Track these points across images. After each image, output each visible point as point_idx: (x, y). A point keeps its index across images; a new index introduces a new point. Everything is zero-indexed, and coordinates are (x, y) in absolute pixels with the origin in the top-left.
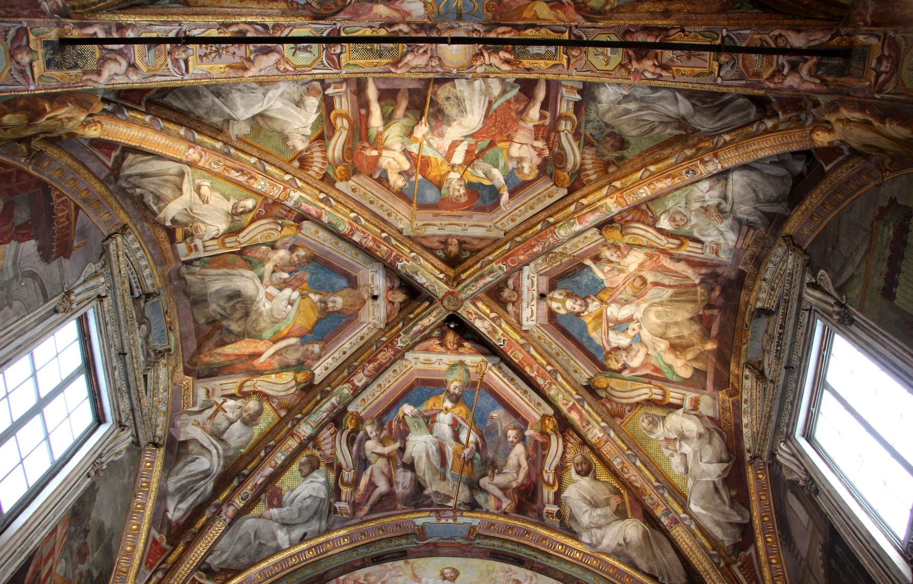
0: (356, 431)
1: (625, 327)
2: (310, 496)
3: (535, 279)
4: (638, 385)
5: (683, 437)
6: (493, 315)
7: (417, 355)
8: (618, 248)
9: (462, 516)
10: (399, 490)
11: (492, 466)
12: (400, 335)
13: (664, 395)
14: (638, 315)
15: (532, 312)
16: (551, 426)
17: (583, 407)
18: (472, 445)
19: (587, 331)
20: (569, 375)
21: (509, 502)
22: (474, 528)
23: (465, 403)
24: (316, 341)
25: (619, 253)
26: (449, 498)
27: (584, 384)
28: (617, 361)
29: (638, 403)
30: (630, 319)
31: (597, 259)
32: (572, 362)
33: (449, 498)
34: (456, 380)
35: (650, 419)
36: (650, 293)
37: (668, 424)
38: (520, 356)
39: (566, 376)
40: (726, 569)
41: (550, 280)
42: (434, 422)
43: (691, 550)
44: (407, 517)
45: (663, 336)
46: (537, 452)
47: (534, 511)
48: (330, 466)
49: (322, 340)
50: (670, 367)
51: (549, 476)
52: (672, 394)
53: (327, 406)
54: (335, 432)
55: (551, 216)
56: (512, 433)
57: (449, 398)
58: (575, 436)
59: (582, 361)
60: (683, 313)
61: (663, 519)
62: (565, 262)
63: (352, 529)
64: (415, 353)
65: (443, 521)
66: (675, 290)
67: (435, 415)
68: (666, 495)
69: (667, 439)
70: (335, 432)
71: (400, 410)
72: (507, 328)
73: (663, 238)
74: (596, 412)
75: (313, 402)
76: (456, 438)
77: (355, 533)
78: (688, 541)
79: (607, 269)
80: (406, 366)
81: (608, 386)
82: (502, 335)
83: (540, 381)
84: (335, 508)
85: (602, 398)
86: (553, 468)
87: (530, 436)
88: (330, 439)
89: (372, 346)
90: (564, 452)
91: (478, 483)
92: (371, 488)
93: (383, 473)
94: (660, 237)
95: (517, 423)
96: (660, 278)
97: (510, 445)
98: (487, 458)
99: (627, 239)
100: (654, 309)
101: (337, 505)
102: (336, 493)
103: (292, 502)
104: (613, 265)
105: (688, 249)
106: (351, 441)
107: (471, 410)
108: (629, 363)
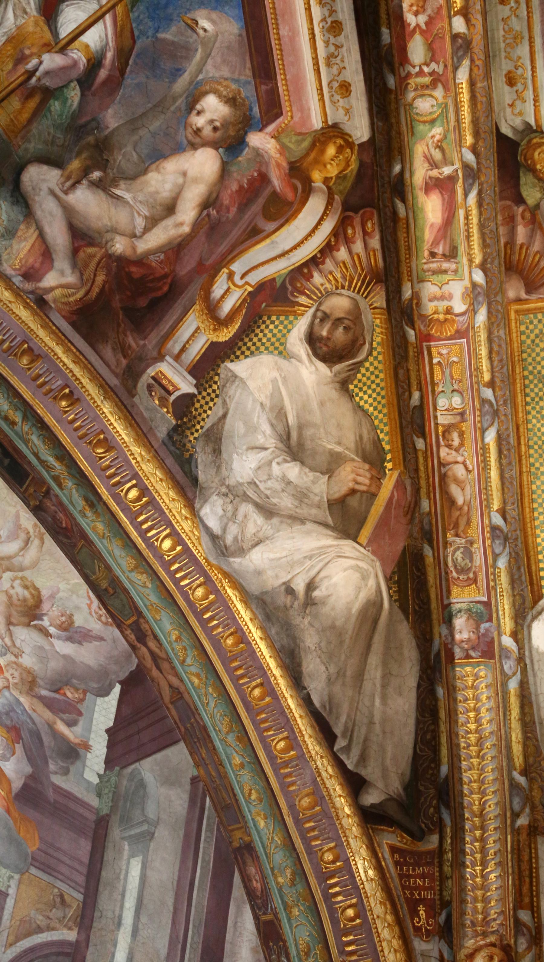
11: (93, 154)
16: (333, 171)
18: (77, 55)
20: (487, 76)
21: (71, 278)
27: (506, 130)
32: (523, 50)
40: (523, 837)
43: (480, 742)
46: (248, 206)
47: (123, 349)
51: (228, 292)
58: (375, 242)
61: (459, 622)
68: (502, 563)
78: (486, 716)
85: (520, 200)
86: (255, 278)
87: (258, 153)
90: (314, 262)
91: (20, 170)
95: (248, 93)
98: (96, 124)
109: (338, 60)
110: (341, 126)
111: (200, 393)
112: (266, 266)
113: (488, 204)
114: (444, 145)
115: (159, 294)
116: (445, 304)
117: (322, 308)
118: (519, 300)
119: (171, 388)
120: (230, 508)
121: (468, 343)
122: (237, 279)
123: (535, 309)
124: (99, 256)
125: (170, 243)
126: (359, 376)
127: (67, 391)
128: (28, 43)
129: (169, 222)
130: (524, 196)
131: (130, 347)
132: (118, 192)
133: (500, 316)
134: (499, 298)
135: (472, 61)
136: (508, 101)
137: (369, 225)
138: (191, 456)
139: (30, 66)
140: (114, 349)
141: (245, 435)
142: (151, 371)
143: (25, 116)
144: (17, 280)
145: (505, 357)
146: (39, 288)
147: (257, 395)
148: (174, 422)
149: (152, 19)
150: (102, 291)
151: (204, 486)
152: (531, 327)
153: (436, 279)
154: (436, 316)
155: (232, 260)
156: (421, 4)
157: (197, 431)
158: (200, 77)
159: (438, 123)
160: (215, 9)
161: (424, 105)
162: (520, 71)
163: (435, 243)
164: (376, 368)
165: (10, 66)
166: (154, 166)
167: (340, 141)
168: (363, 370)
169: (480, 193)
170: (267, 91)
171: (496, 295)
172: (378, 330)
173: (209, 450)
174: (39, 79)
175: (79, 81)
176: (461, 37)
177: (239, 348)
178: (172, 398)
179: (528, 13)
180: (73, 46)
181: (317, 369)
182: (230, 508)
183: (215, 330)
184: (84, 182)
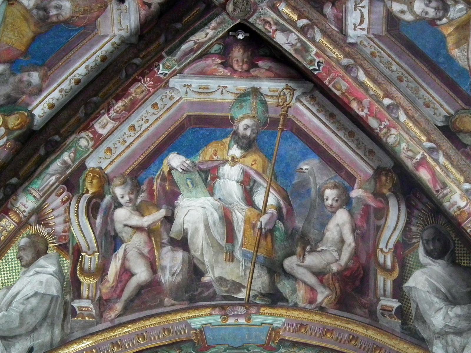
0: (100, 195)
2: (36, 294)
6: (302, 22)
7: (188, 81)
9: (258, 313)
10: (166, 278)
11: (302, 241)
12: (161, 58)
15: (362, 16)
16: (389, 185)
17: (437, 161)
18: (271, 211)
19: (445, 47)
21: (327, 292)
22: (275, 330)
23: (261, 150)
24: (34, 67)
26: (239, 287)
27: (440, 124)
32: (422, 92)
33: (239, 287)
34: (248, 116)
38: (344, 85)
39: (412, 111)
42: (216, 177)
44: (178, 316)
47: (363, 306)
48: (63, 248)
49: (43, 65)
53: (57, 165)
54: (69, 199)
56: (330, 194)
57: (237, 143)
58: (425, 200)
59: (436, 91)
63: (99, 338)
64: (185, 77)
65: (231, 321)
67: (217, 168)
70: (69, 199)
71: (165, 162)
72: (325, 42)
74: (456, 167)
75: (34, 159)
76: (249, 199)
77: (103, 344)
80: (171, 98)
82: (317, 54)
83: (373, 123)
84: (73, 308)
87: (358, 198)
88: (62, 209)
89: (119, 72)
91: (282, 265)
92: (125, 277)
93: (141, 254)
95: (339, 180)
97: (328, 211)
98: (295, 229)
101: (76, 304)
102: (73, 286)
103: (10, 304)
106: (92, 210)
107: (270, 160)
109: (361, 144)
110: (380, 166)
111: (402, 303)
112: (392, 238)
113: (454, 155)
115: (361, 276)
116: (456, 206)
117: (423, 239)
119: (390, 309)
120: (444, 341)
122: (385, 250)
124: (330, 277)
125: (351, 254)
126: (457, 255)
127: (351, 337)
128: (252, 219)
129: (345, 246)
130: (466, 143)
131: (365, 303)
132: (320, 249)
138: (415, 330)
139: (259, 226)
140: (360, 309)
141: (430, 308)
142: (379, 307)
143: (270, 244)
144: (308, 307)
146: (318, 304)
147: (424, 290)
148: (400, 321)
149: (286, 179)
150: (341, 290)
151: (428, 339)
153: (445, 199)
155: (378, 244)
157: (411, 319)
158: (318, 187)
159: (401, 142)
160: (304, 159)
162: (427, 100)
163: (435, 186)
164: (461, 247)
165: (252, 231)
166: (325, 230)
168: (457, 252)
170: (345, 174)
172: (451, 232)
173: (420, 323)
174: (265, 229)
175: (279, 219)
176: (391, 105)
177: (405, 276)
178: (393, 312)
179: (413, 78)
180: (267, 209)
181: (438, 263)
182: (444, 341)
183: (391, 275)
184: (306, 253)
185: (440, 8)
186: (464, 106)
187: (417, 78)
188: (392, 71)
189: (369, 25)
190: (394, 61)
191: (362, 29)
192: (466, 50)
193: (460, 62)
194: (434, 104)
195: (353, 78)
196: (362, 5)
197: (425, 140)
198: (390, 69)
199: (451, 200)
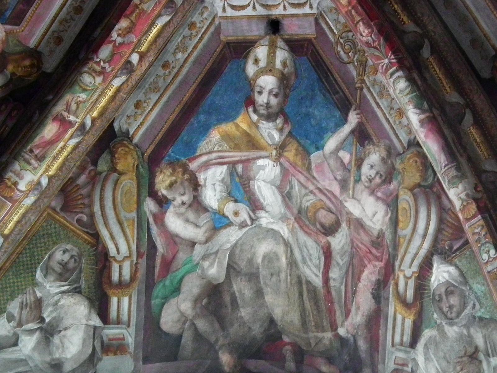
1: (238, 196)
3: (306, 10)
4: (132, 232)
5: (49, 332)
8: (388, 178)
13: (121, 285)
14: (265, 220)
15: (242, 8)
16: (20, 72)
19: (220, 121)
20: (129, 93)
25: (378, 180)
27: (116, 126)
28: (171, 186)
29: (96, 236)
30: (255, 206)
31: (362, 136)
32: (154, 97)
35: (71, 265)
36: (310, 242)
37: (67, 301)
41: (309, 41)
45: (232, 269)
50: (177, 290)
52: (126, 300)
55: (434, 50)
58: (11, 123)
59: (159, 115)
60: (280, 306)
62: (348, 72)
66: (322, 291)
69: (38, 303)
73: (415, 268)
79: (345, 156)
81: (121, 174)
85: (95, 163)
94: (417, 263)
96: (340, 260)
99: (406, 198)
100: (281, 250)
104: (353, 169)
105: (399, 318)
108: (171, 209)
110: (42, 55)
113: (79, 152)
114: (81, 105)
116: (17, 179)
118: (54, 209)
121: (12, 207)
123: (58, 220)
130: (99, 163)
133: (38, 209)
134: (45, 200)
135: (127, 80)
136: (129, 112)
137: (15, 112)
145: (24, 230)
152: (49, 227)
153: (23, 164)
154: (7, 181)
156: (125, 33)
159: (87, 93)
161: (87, 79)
162: (145, 105)
163: (37, 147)
167: (35, 62)
169: (79, 143)
171: (45, 197)
176: (131, 65)
179: (171, 82)
185: (270, 110)
186: (146, 155)
187: (173, 87)
188: (174, 54)
189: (232, 18)
190: (189, 56)
191: (224, 9)
192: (220, 149)
193: (204, 143)
194: (141, 114)
195: (160, 11)
196: (257, 6)
197: (92, 116)
198: (177, 51)
199: (23, 172)
